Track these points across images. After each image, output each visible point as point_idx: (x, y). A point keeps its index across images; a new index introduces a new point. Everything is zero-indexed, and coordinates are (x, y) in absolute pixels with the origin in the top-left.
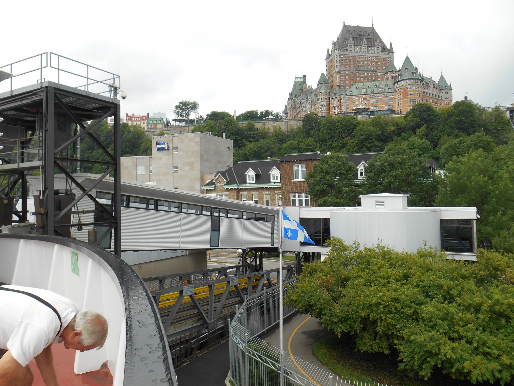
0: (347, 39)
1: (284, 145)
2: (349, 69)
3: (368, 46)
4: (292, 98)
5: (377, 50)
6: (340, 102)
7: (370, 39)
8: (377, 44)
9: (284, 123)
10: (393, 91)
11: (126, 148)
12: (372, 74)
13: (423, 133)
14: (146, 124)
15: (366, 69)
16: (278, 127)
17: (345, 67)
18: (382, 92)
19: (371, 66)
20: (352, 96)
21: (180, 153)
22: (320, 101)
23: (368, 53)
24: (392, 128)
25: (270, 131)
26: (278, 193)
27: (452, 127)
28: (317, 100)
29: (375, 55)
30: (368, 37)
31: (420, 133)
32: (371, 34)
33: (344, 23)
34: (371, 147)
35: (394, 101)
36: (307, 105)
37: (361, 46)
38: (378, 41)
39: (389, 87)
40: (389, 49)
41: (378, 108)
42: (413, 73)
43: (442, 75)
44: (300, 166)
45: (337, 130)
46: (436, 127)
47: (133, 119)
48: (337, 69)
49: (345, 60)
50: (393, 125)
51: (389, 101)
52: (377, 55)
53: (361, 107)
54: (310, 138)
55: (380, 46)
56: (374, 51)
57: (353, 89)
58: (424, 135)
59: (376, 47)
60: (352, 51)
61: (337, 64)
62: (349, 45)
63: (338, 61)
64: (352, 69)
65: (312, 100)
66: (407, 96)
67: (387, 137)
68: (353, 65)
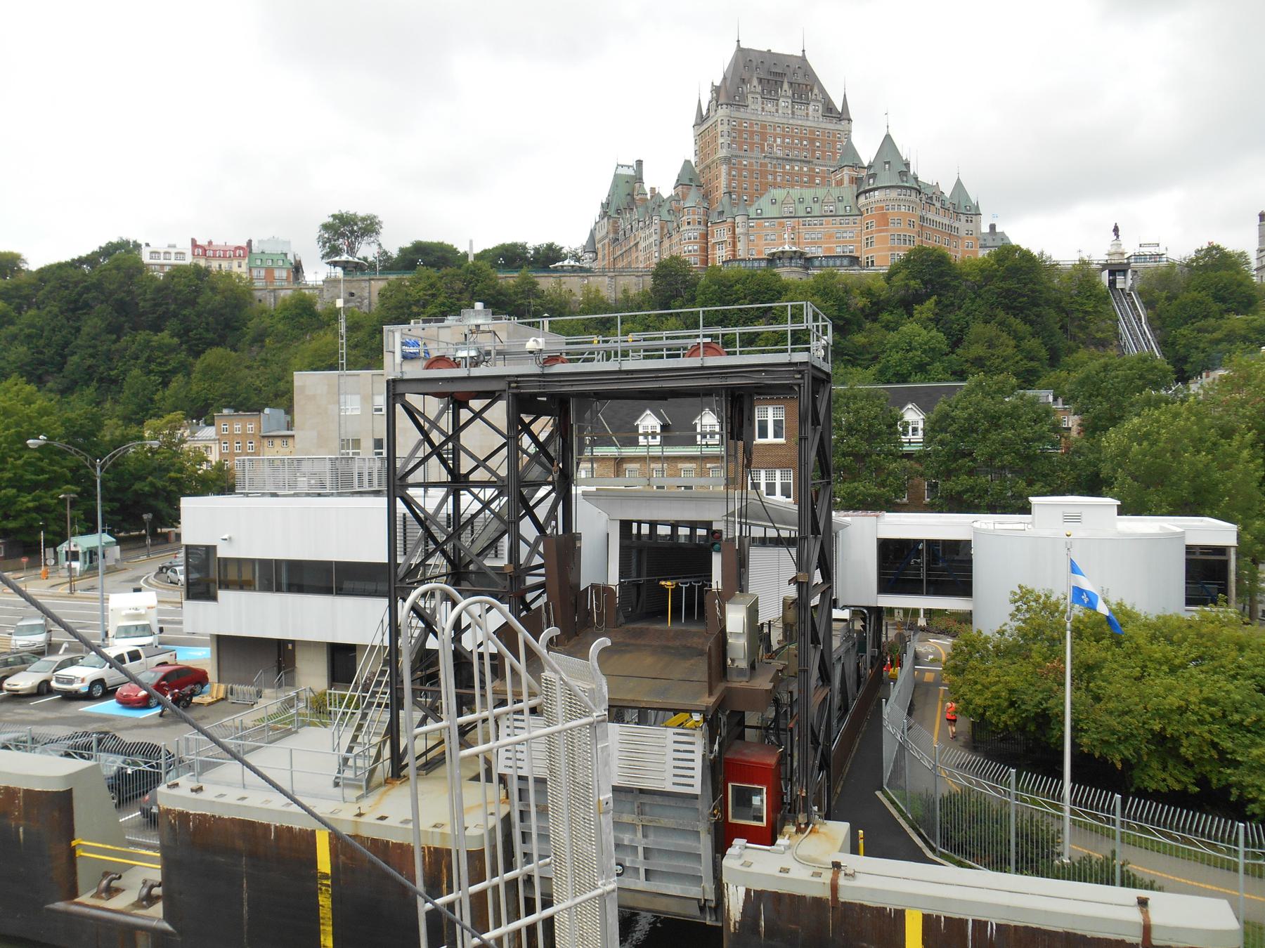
0: (746, 80)
2: (748, 154)
3: (793, 102)
4: (609, 213)
6: (734, 233)
7: (799, 84)
8: (814, 97)
9: (607, 279)
10: (855, 212)
11: (207, 330)
12: (801, 169)
13: (930, 315)
14: (244, 268)
15: (788, 155)
16: (593, 289)
17: (740, 149)
18: (831, 214)
19: (799, 148)
20: (763, 221)
22: (686, 227)
23: (792, 118)
24: (860, 302)
25: (574, 298)
26: (713, 468)
27: (993, 304)
28: (675, 224)
29: (809, 124)
30: (793, 81)
31: (924, 316)
32: (800, 73)
33: (738, 41)
35: (858, 237)
36: (650, 235)
37: (778, 100)
38: (816, 91)
39: (845, 203)
40: (840, 110)
41: (820, 250)
43: (958, 179)
44: (770, 410)
46: (957, 302)
47: (210, 253)
48: (723, 153)
49: (741, 132)
50: (862, 294)
51: (845, 235)
52: (813, 125)
53: (787, 248)
55: (820, 102)
56: (807, 114)
57: (764, 202)
58: (930, 320)
59: (812, 103)
60: (758, 110)
61: (723, 141)
62: (750, 96)
64: (756, 153)
65: (664, 223)
66: (888, 225)
67: (848, 322)
68: (760, 144)
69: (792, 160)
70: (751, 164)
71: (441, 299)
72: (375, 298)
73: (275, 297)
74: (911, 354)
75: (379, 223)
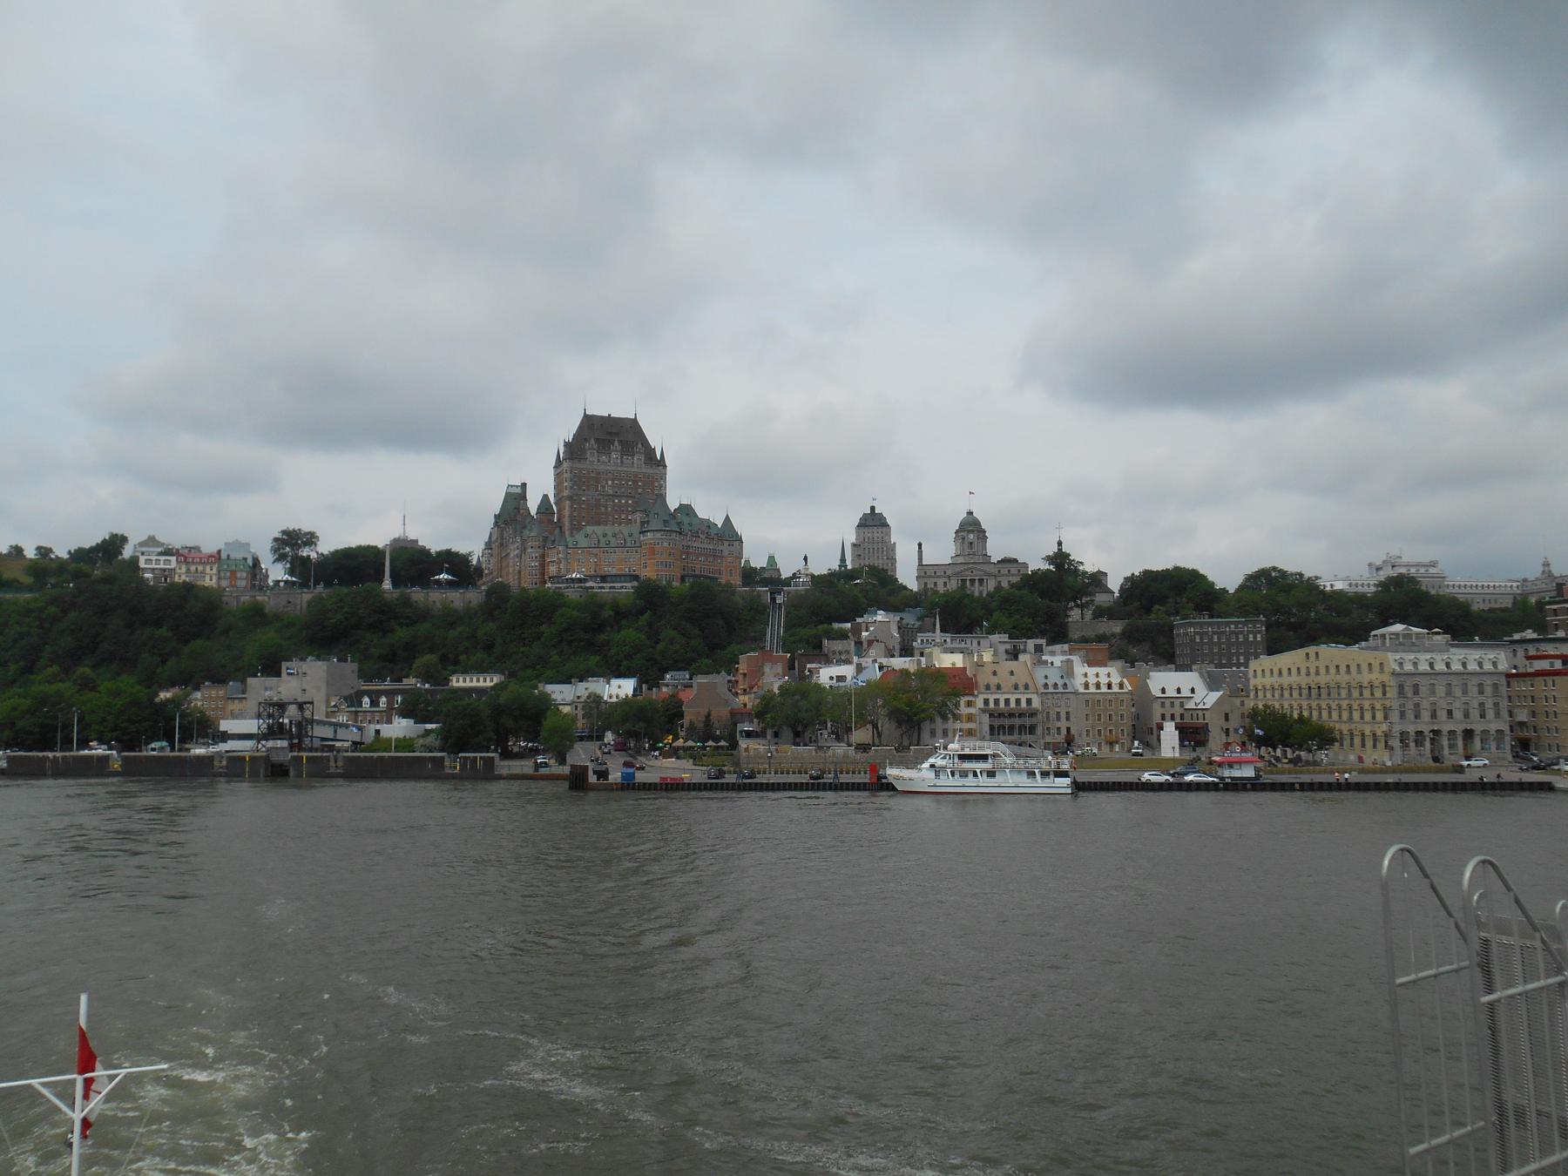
1: (453, 634)
5: (638, 460)
12: (627, 502)
14: (214, 571)
17: (580, 489)
21: (308, 678)
22: (530, 550)
34: (572, 641)
36: (514, 551)
38: (640, 446)
42: (665, 521)
45: (532, 612)
48: (566, 493)
53: (574, 576)
54: (491, 624)
56: (633, 463)
60: (594, 461)
62: (589, 452)
63: (568, 480)
65: (524, 542)
69: (618, 496)
70: (588, 500)
71: (346, 609)
72: (305, 605)
73: (237, 602)
74: (624, 649)
75: (317, 537)
